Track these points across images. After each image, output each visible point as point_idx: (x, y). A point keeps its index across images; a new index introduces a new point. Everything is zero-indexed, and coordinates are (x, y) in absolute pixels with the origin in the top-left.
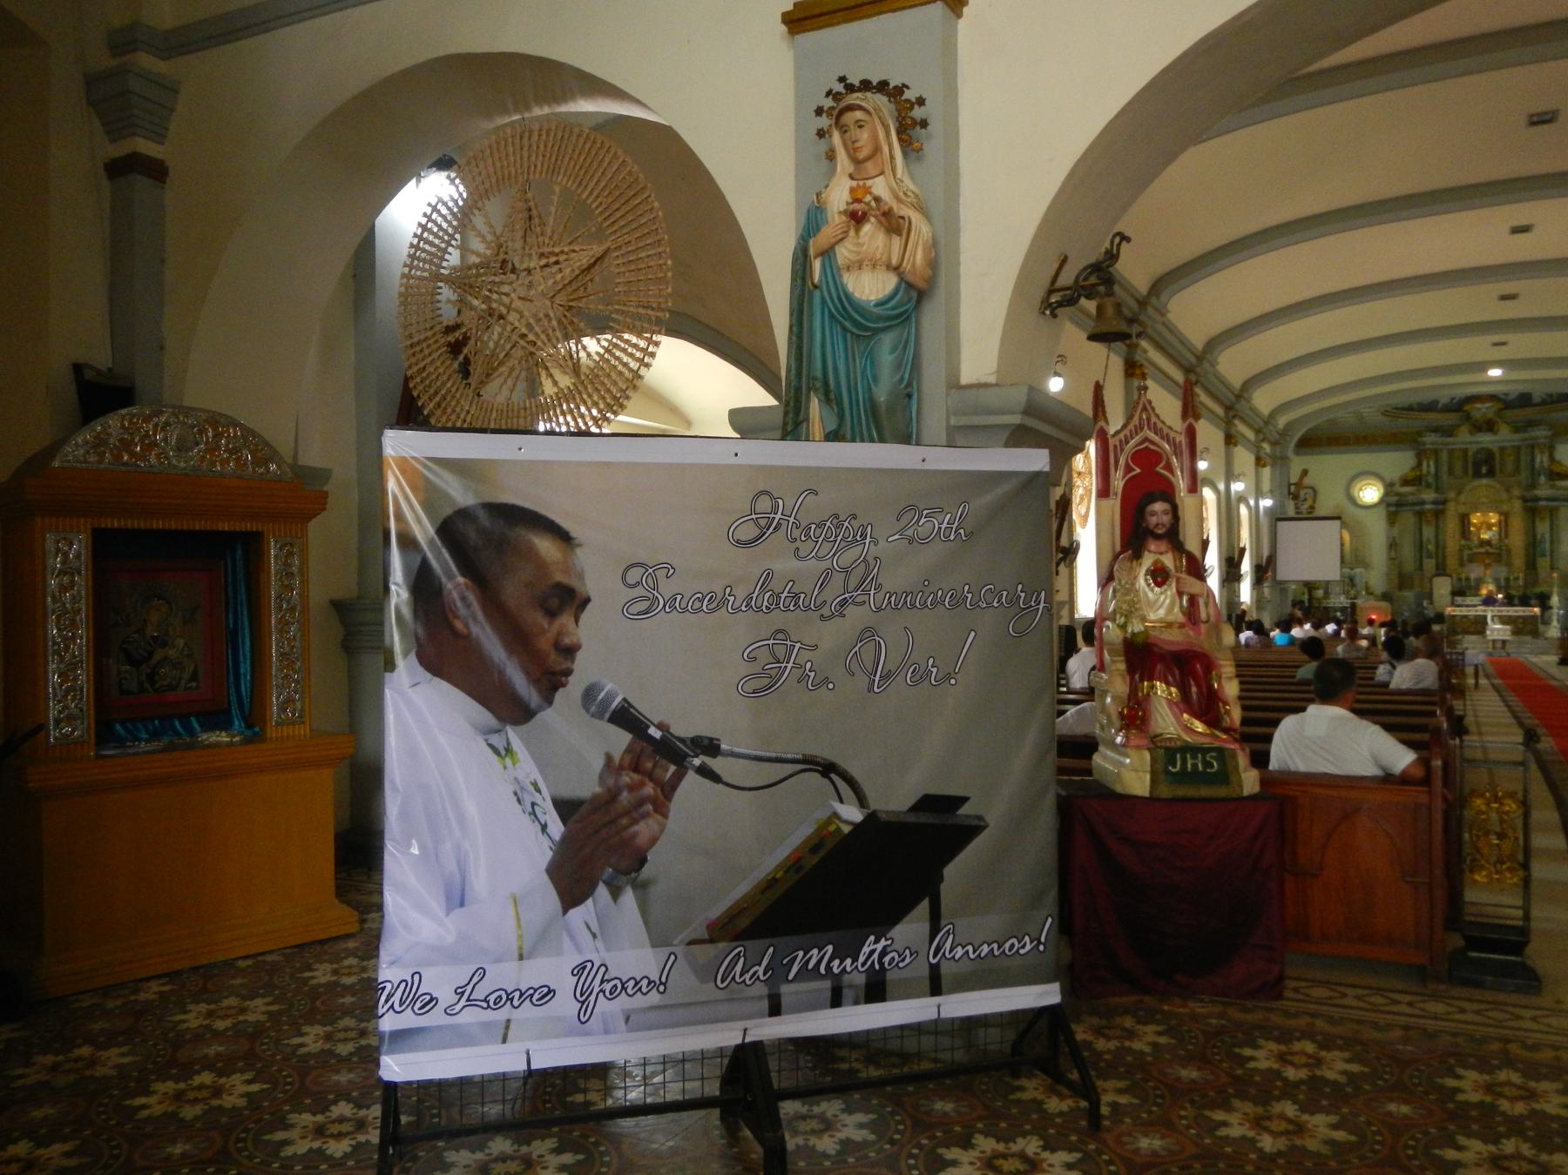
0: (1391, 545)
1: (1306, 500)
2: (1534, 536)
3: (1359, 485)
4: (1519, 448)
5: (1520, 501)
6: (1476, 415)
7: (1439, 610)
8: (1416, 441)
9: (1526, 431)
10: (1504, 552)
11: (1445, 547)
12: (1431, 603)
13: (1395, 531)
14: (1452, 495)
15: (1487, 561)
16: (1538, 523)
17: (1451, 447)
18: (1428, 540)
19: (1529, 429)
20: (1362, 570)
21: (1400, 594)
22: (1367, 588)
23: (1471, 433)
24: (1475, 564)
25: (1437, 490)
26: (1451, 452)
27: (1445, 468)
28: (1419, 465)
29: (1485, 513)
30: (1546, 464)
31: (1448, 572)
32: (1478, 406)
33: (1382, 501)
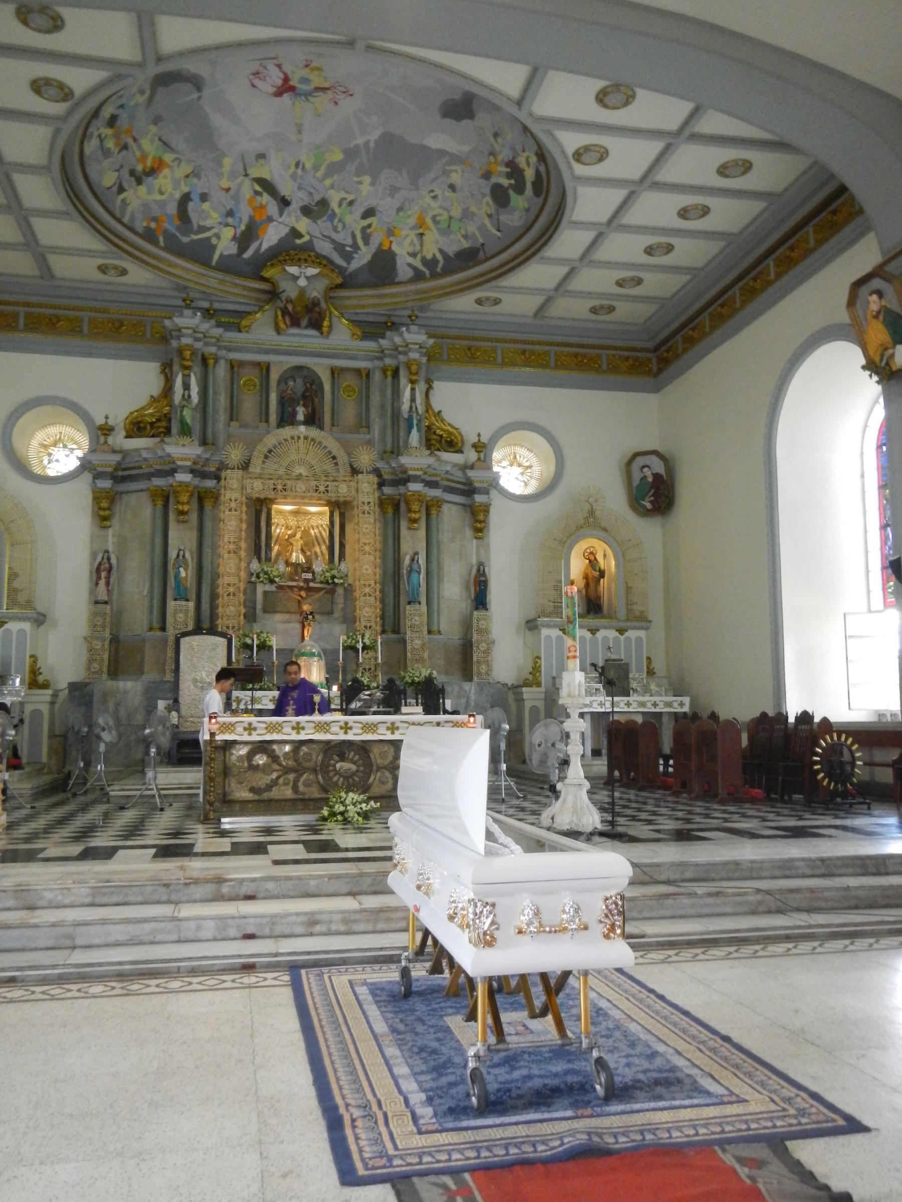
0: (98, 570)
2: (398, 562)
3: (41, 436)
4: (367, 375)
5: (374, 479)
6: (289, 290)
7: (187, 727)
8: (165, 338)
9: (383, 337)
10: (340, 590)
11: (215, 576)
12: (175, 704)
14: (235, 455)
15: (306, 608)
16: (404, 531)
17: (234, 356)
18: (181, 559)
19: (388, 333)
20: (26, 626)
21: (111, 684)
22: (35, 672)
23: (278, 331)
24: (278, 617)
25: (204, 443)
26: (234, 367)
27: (223, 401)
28: (168, 390)
29: (303, 499)
30: (421, 409)
31: (221, 625)
32: (293, 270)
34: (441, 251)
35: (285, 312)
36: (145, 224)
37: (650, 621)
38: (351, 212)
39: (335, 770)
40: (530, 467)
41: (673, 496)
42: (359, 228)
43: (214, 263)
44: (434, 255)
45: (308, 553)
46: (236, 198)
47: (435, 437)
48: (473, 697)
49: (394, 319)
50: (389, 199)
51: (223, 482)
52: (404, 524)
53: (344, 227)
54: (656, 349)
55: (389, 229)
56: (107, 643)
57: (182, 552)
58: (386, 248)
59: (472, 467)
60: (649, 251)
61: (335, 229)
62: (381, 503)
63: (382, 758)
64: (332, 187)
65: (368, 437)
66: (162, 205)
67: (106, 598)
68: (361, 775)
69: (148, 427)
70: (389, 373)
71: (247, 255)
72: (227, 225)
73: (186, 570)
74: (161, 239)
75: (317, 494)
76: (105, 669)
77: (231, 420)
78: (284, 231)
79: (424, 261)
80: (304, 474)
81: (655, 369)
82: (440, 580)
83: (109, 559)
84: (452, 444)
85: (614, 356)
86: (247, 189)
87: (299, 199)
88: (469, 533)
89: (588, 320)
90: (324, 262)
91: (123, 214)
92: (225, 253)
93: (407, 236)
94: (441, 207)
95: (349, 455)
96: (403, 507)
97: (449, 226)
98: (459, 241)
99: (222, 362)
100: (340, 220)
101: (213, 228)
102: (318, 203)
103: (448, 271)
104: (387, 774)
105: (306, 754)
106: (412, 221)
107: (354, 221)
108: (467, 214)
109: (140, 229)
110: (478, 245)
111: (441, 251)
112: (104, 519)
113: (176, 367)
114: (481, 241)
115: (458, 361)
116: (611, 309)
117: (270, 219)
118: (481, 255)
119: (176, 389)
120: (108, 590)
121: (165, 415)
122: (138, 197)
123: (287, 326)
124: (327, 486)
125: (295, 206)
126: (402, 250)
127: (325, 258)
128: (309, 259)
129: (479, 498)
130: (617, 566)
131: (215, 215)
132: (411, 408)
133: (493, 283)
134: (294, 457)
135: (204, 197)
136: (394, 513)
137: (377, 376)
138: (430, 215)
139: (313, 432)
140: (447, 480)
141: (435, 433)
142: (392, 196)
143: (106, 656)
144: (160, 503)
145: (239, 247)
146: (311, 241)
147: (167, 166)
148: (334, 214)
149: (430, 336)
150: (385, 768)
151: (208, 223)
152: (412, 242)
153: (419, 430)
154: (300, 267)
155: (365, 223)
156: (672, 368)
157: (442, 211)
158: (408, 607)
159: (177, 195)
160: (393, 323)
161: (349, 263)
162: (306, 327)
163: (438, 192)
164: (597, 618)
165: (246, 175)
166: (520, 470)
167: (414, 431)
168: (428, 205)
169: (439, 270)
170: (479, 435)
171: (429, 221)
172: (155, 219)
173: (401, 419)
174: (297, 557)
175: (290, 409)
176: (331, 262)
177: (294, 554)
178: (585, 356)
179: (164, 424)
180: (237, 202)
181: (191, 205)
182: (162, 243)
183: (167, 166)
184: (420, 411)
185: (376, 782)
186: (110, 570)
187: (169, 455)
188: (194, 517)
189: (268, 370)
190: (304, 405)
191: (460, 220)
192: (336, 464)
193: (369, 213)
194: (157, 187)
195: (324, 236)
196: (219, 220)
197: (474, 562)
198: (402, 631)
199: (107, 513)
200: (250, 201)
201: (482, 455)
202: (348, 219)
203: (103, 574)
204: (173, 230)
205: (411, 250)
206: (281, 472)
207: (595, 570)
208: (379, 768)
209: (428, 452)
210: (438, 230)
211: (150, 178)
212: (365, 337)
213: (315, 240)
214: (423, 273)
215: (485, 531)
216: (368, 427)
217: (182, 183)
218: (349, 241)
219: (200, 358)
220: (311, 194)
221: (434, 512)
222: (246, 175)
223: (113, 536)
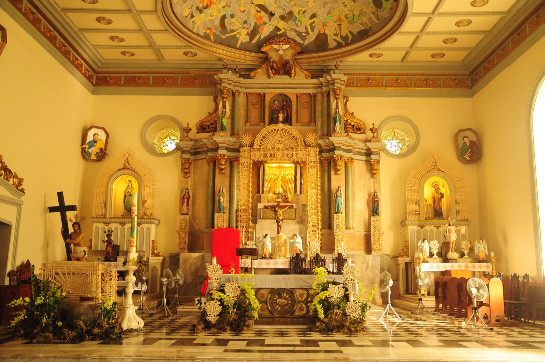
0: (183, 199)
1: (95, 142)
4: (312, 97)
6: (274, 56)
9: (322, 77)
13: (190, 184)
14: (246, 140)
16: (333, 177)
19: (324, 75)
23: (269, 77)
25: (232, 134)
26: (247, 95)
28: (216, 110)
29: (281, 160)
32: (276, 47)
33: (178, 148)
34: (350, 32)
35: (272, 68)
36: (204, 31)
37: (470, 221)
38: (304, 17)
39: (276, 302)
40: (403, 139)
41: (482, 153)
42: (309, 24)
43: (238, 47)
44: (347, 34)
45: (285, 188)
46: (248, 15)
47: (350, 126)
48: (370, 263)
49: (328, 68)
50: (323, 8)
51: (241, 154)
52: (333, 173)
53: (301, 24)
54: (470, 74)
55: (323, 23)
56: (187, 234)
57: (221, 189)
58: (322, 32)
59: (370, 141)
60: (458, 24)
61: (297, 25)
62: (321, 162)
63: (300, 297)
64: (295, 5)
65: (315, 127)
66: (212, 21)
67: (186, 212)
68: (289, 305)
69: (207, 128)
70: (325, 95)
71: (254, 41)
72: (244, 28)
73: (223, 198)
74: (212, 37)
75: (288, 158)
76: (186, 247)
77: (247, 122)
78: (272, 28)
79: (342, 37)
80: (281, 148)
81: (470, 85)
82: (354, 200)
83: (188, 193)
84: (358, 129)
85: (447, 79)
86: (253, 10)
87: (278, 12)
88: (368, 176)
89: (431, 61)
90: (292, 42)
91: (194, 28)
92: (243, 42)
93: (333, 25)
94: (348, 10)
95: (304, 137)
96: (332, 164)
97: (353, 19)
98: (359, 26)
99: (242, 94)
100: (299, 21)
101: (237, 30)
102: (288, 13)
103: (353, 42)
104: (304, 306)
105: (262, 294)
106: (335, 18)
107: (306, 21)
108: (362, 13)
109: (202, 34)
110: (368, 28)
111: (350, 32)
112: (186, 173)
113: (219, 98)
114: (370, 25)
115: (361, 86)
116: (443, 55)
117: (265, 23)
118: (370, 33)
119: (219, 109)
120: (188, 208)
121: (215, 121)
122: (200, 19)
123: (273, 75)
124: (293, 154)
125: (277, 16)
126: (330, 32)
127: (292, 39)
128: (284, 41)
129: (373, 157)
130: (450, 191)
131: (238, 24)
132: (336, 112)
133: (377, 47)
134: (276, 139)
135: (232, 16)
136: (328, 166)
137: (319, 97)
138: (344, 14)
139: (287, 127)
140: (356, 148)
141: (350, 124)
142: (324, 7)
143: (187, 241)
144: (211, 164)
145: (250, 38)
146: (285, 32)
147: (214, 3)
148: (296, 18)
149: (345, 74)
150: (302, 302)
151: (234, 28)
152: (335, 29)
153: (340, 123)
154: (279, 45)
155: (311, 21)
156: (479, 83)
157: (349, 12)
158: (335, 215)
159: (220, 16)
160: (327, 69)
161: (304, 41)
162: (283, 75)
163: (347, 3)
164: (440, 219)
165: (253, 3)
166: (398, 141)
167: (338, 124)
168: (342, 9)
169: (349, 41)
170: (373, 124)
171: (343, 18)
172: (209, 29)
173: (331, 118)
174: (279, 190)
175: (275, 115)
176: (295, 41)
177: (277, 189)
178: (430, 80)
179: (213, 126)
180: (249, 17)
181: (226, 20)
182: (213, 40)
183: (214, 3)
184: (341, 114)
185: (298, 309)
186: (188, 198)
187: (215, 141)
188: (228, 170)
189: (265, 96)
190: (282, 113)
191: (359, 16)
192: (297, 142)
193: (313, 16)
194: (210, 13)
195: (291, 29)
196: (240, 26)
197: (372, 191)
198: (332, 228)
199: (188, 170)
200: (255, 16)
201: (375, 135)
202: (303, 20)
203: (186, 200)
204: (218, 33)
205: (335, 33)
206: (269, 147)
207: (438, 194)
208: (299, 302)
209: (346, 134)
210: (347, 21)
211: (206, 10)
212: (313, 77)
213: (287, 31)
214: (342, 43)
215: (377, 174)
216: (315, 122)
217: (222, 10)
218: (304, 30)
219: (231, 92)
220: (284, 9)
221: (350, 165)
222: (253, 3)
223: (191, 181)
